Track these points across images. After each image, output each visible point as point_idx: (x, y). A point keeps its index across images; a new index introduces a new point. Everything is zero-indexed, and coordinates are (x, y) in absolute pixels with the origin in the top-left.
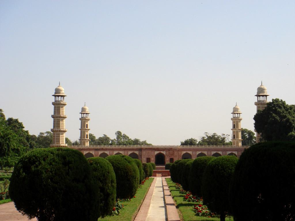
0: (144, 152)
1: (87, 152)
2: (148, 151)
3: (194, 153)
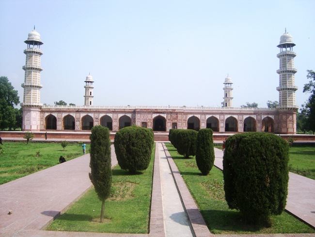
0: (139, 115)
3: (203, 116)
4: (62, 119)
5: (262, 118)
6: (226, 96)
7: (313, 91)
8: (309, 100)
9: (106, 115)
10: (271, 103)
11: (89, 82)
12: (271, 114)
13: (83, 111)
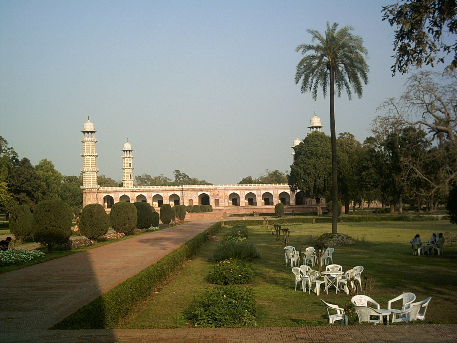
1: (123, 194)
2: (189, 192)
3: (242, 192)
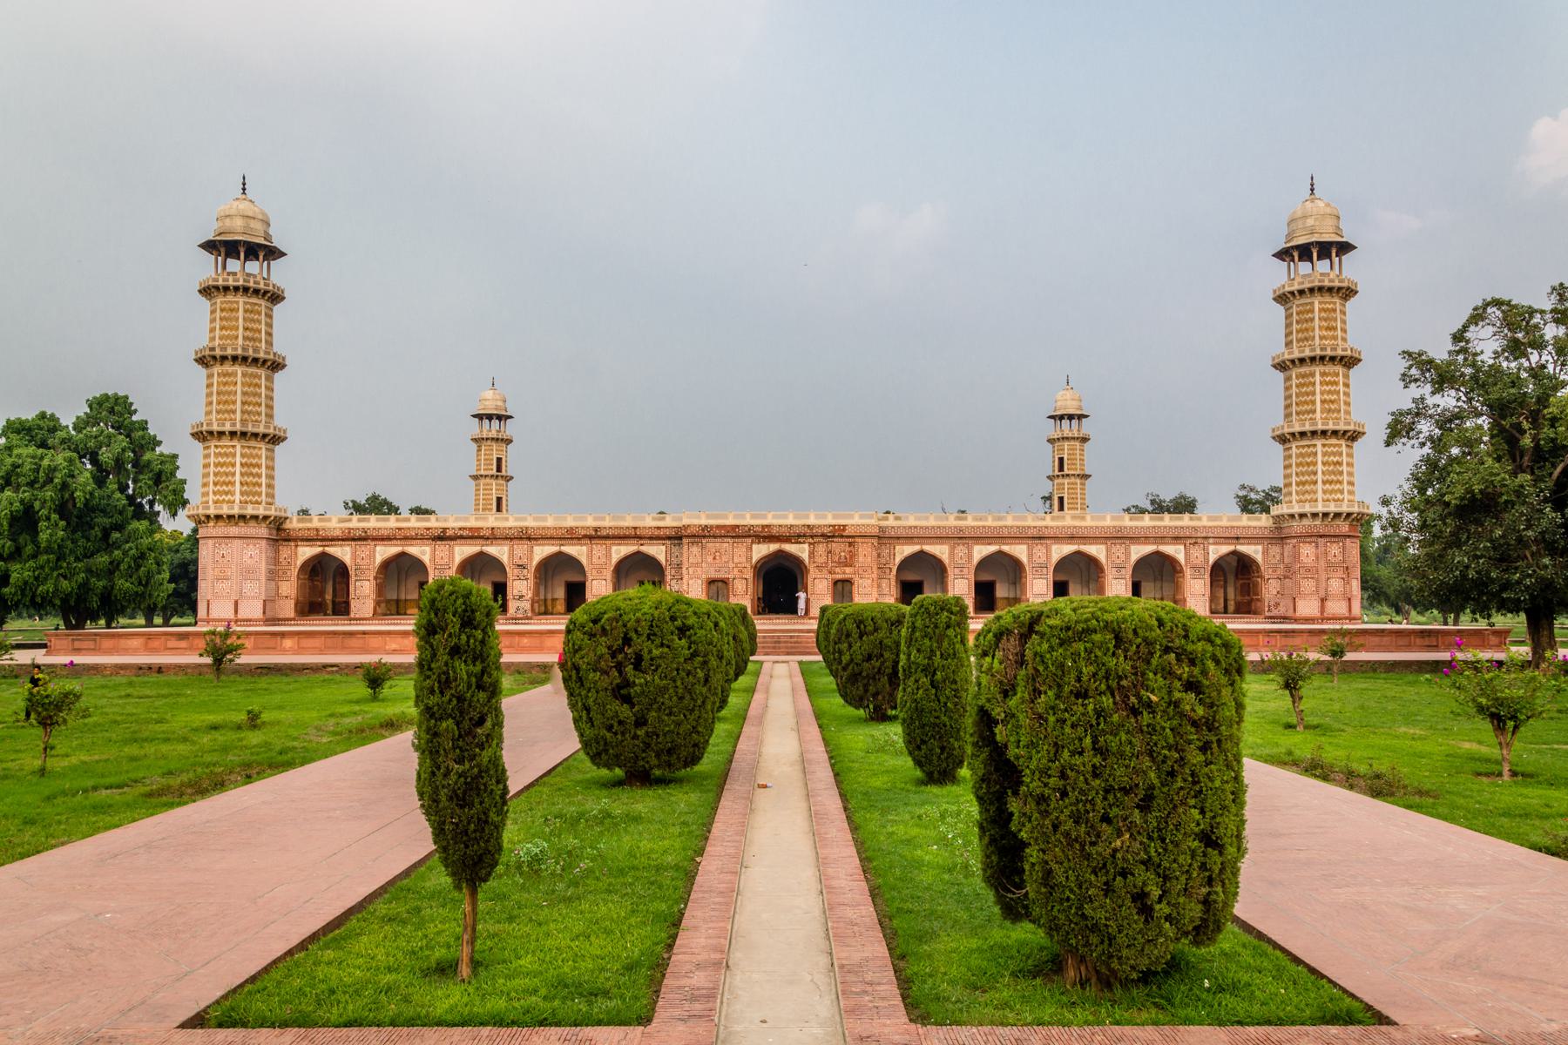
0: (695, 549)
2: (712, 545)
3: (961, 550)
4: (373, 574)
5: (1212, 558)
6: (1061, 468)
7: (1431, 438)
8: (1415, 477)
9: (560, 553)
10: (1253, 496)
11: (490, 417)
12: (1252, 539)
13: (461, 537)
